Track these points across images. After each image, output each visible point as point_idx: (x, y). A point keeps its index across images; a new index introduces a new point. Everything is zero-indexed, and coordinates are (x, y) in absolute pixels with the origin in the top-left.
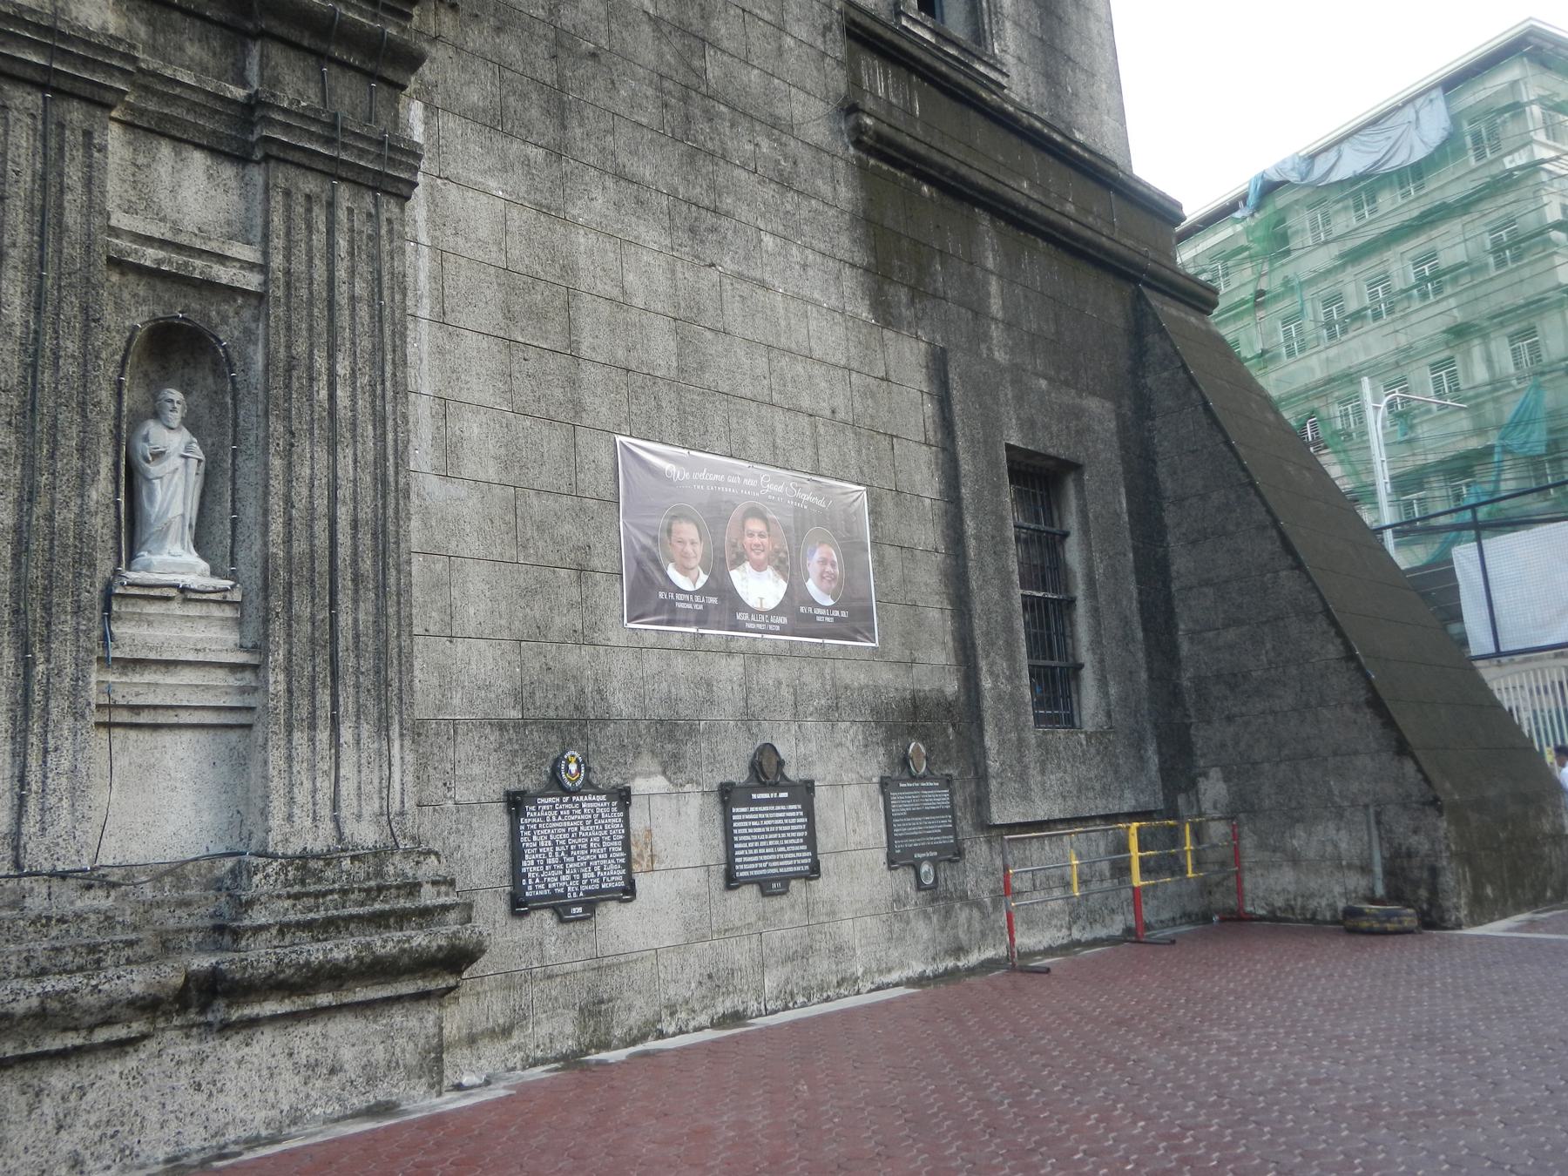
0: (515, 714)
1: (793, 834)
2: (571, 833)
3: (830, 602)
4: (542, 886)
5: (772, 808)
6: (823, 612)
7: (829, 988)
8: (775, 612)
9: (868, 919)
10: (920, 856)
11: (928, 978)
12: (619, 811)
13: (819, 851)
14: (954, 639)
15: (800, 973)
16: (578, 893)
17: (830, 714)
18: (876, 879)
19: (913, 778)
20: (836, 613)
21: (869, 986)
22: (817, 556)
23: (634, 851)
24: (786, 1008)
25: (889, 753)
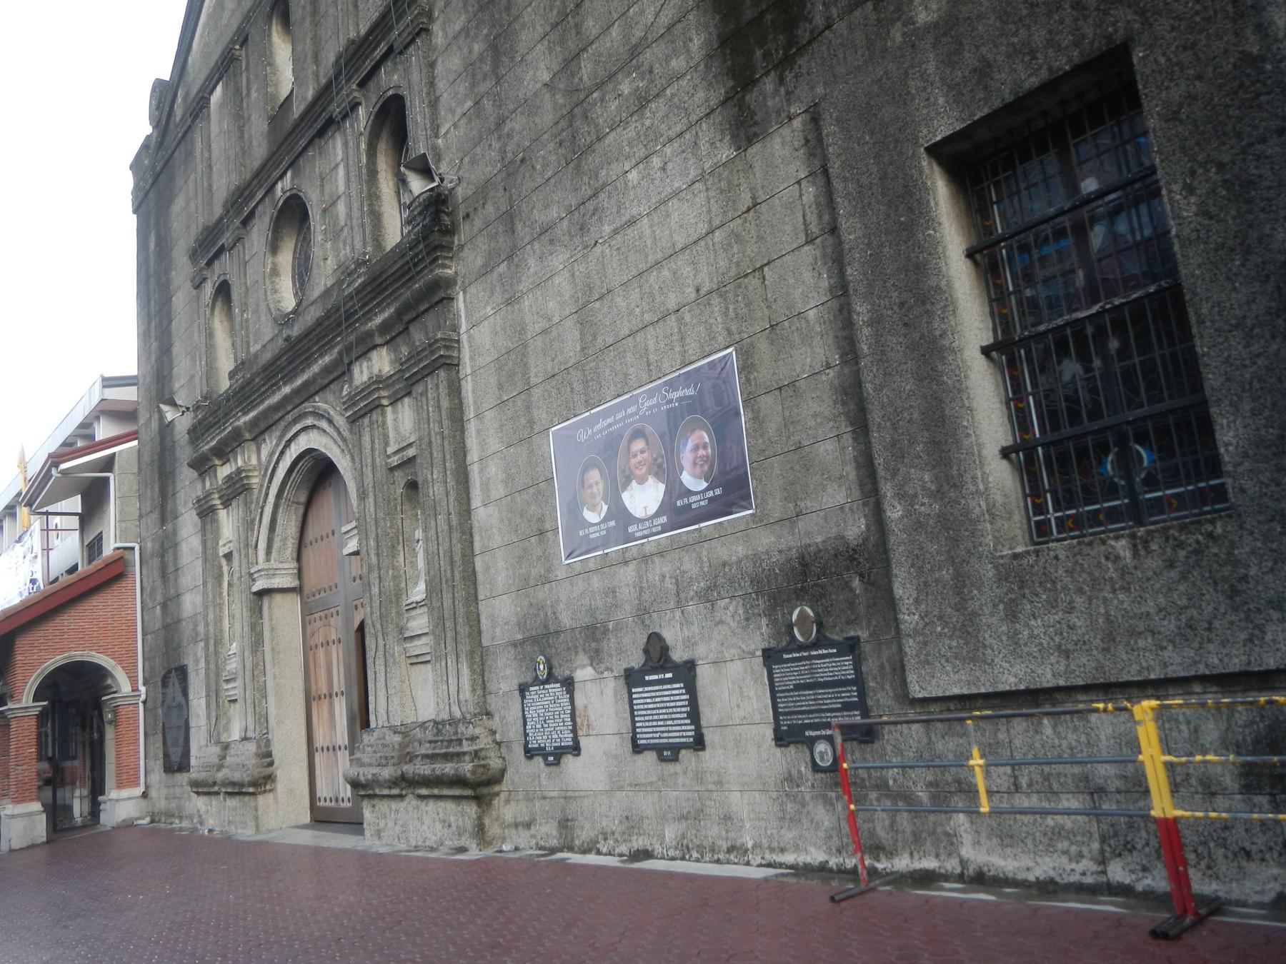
0: (520, 637)
1: (679, 710)
3: (705, 485)
5: (660, 687)
6: (697, 498)
7: (719, 851)
8: (658, 514)
9: (757, 794)
10: (813, 733)
11: (831, 870)
13: (704, 723)
14: (858, 468)
15: (694, 832)
17: (708, 597)
18: (764, 755)
19: (801, 648)
20: (711, 494)
21: (759, 861)
22: (690, 445)
23: (578, 720)
24: (683, 859)
25: (773, 622)
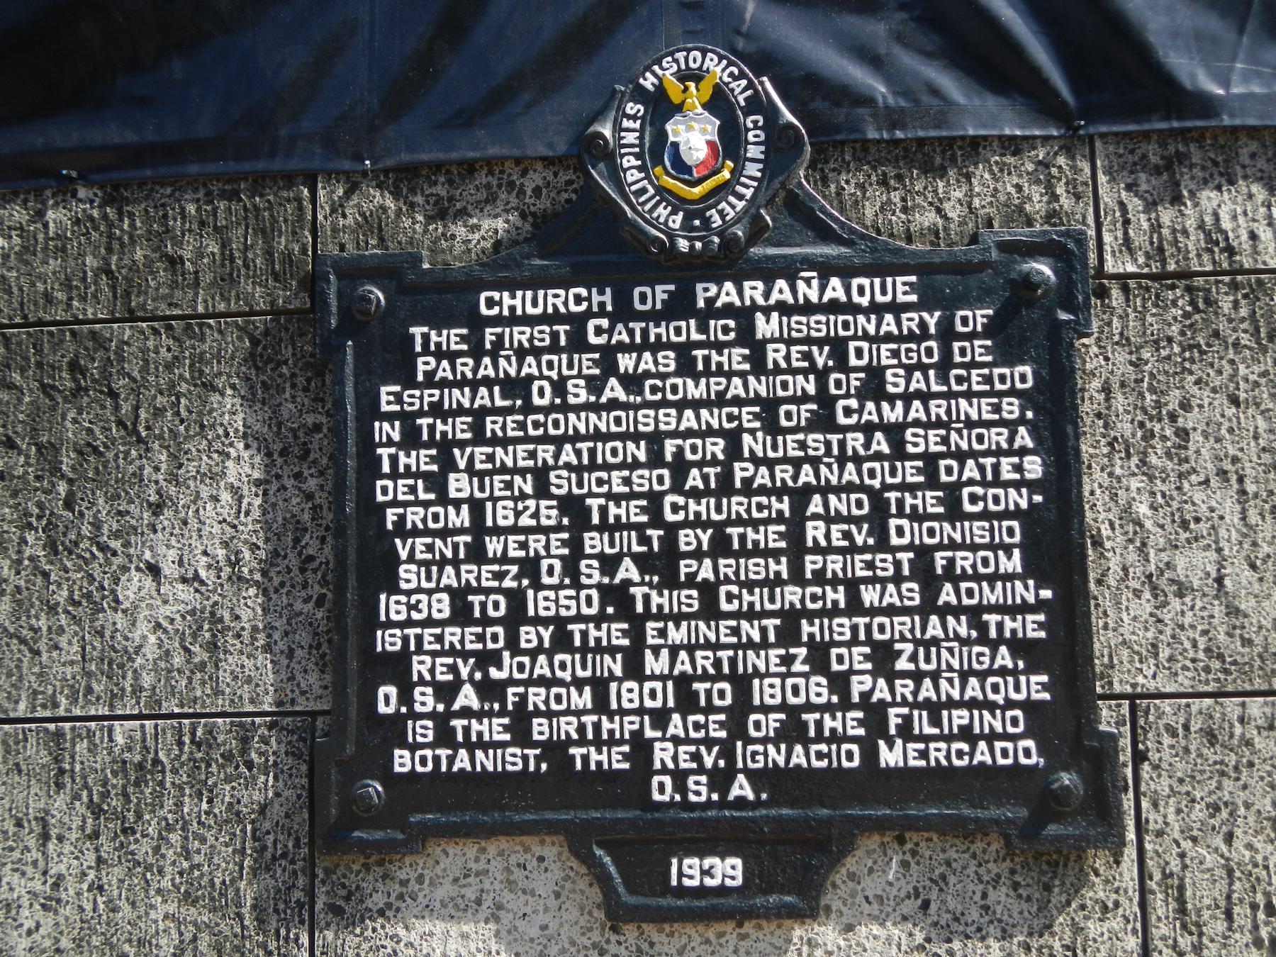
2: (680, 468)
4: (496, 729)
12: (1007, 354)
16: (721, 780)
